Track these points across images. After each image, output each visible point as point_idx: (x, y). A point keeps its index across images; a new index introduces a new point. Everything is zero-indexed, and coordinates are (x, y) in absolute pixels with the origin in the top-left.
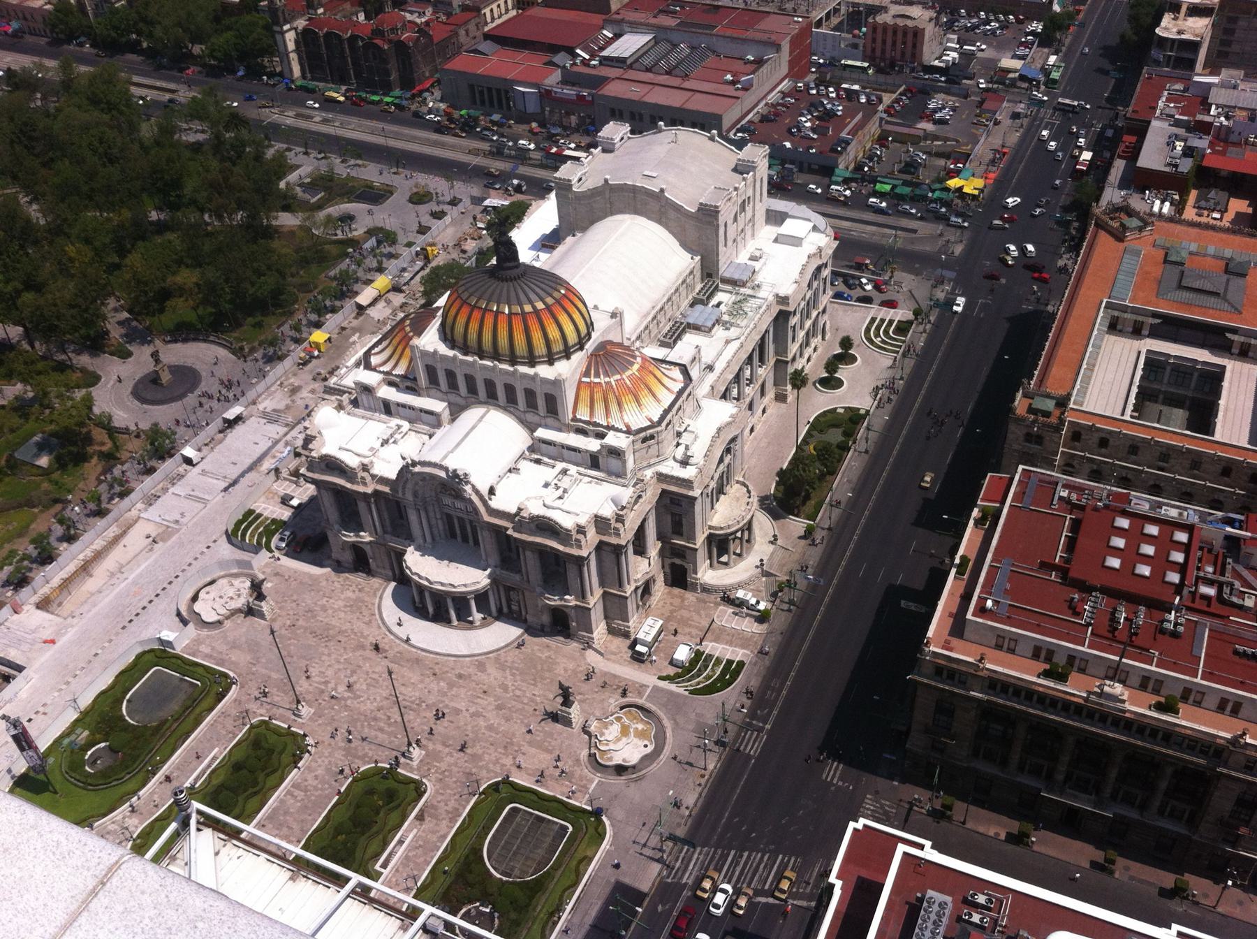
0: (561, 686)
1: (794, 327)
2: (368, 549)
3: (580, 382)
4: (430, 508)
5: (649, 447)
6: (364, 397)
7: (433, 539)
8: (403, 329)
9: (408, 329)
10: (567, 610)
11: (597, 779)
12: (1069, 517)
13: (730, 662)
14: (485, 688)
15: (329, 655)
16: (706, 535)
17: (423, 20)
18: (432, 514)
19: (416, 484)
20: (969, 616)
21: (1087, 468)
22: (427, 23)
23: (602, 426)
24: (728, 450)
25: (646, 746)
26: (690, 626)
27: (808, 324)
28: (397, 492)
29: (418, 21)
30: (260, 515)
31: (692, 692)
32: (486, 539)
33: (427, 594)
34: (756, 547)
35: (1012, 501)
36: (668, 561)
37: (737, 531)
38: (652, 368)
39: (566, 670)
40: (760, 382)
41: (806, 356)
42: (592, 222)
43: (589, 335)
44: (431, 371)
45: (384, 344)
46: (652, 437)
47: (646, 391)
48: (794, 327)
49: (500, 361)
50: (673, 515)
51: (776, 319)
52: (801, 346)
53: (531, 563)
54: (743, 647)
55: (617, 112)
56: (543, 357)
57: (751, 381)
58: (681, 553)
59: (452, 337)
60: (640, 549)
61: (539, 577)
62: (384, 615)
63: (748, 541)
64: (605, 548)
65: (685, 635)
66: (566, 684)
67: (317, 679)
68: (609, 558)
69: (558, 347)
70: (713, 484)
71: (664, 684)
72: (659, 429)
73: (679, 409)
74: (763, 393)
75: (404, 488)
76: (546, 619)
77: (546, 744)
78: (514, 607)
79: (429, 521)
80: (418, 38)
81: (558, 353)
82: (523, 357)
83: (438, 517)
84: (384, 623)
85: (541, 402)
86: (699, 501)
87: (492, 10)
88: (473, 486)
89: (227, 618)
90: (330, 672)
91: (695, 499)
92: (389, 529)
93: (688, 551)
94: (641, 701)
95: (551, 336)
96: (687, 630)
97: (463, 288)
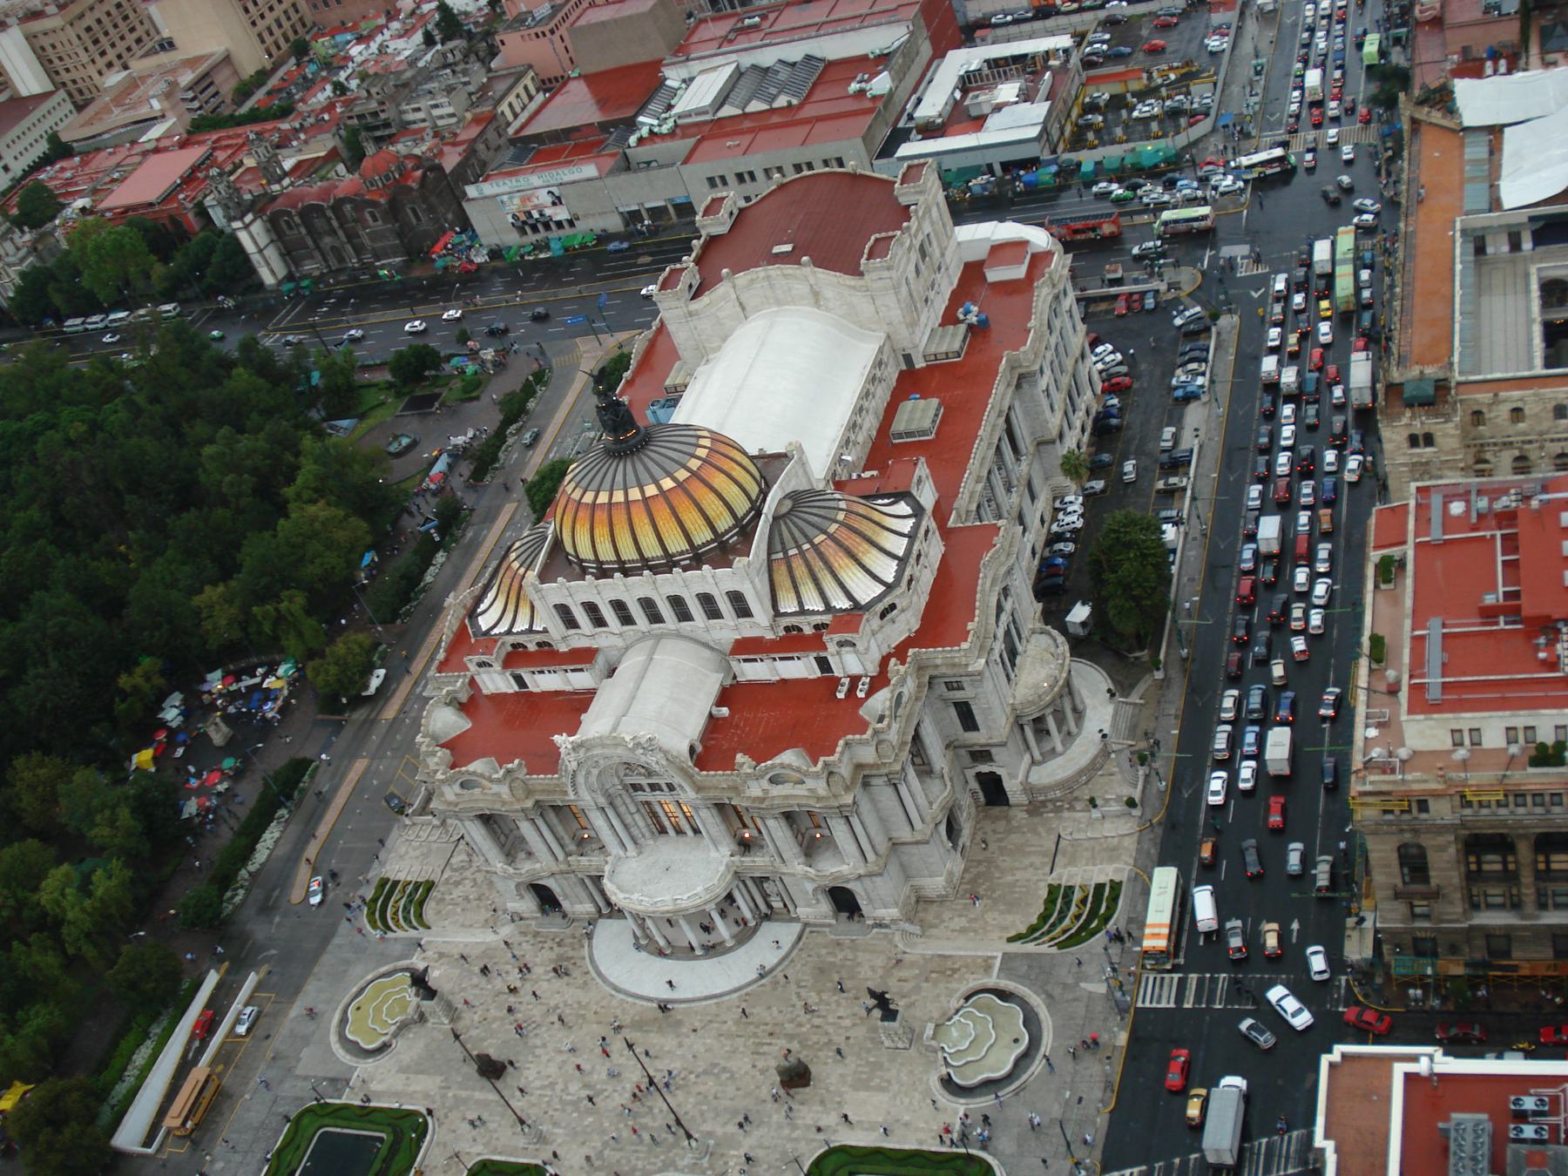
0: (872, 994)
1: (1047, 391)
2: (550, 883)
3: (770, 562)
4: (618, 802)
5: (894, 622)
6: (484, 676)
7: (636, 843)
8: (509, 567)
9: (516, 565)
10: (849, 886)
11: (960, 1106)
12: (1498, 533)
13: (1099, 888)
14: (769, 1028)
15: (544, 1045)
16: (1011, 719)
17: (424, 148)
18: (622, 809)
19: (588, 773)
20: (1404, 717)
21: (1507, 457)
22: (430, 149)
23: (818, 613)
24: (1005, 592)
25: (1016, 1041)
26: (1029, 853)
27: (1065, 380)
28: (566, 793)
29: (417, 151)
30: (396, 883)
31: (1061, 946)
32: (708, 820)
33: (649, 923)
34: (1089, 713)
35: (1416, 536)
36: (970, 773)
37: (1053, 701)
38: (862, 510)
39: (873, 969)
40: (1024, 482)
41: (1078, 424)
42: (724, 339)
43: (764, 494)
44: (564, 612)
45: (491, 595)
46: (893, 607)
47: (866, 546)
48: (1047, 391)
49: (650, 568)
50: (956, 705)
51: (1018, 386)
52: (1066, 413)
53: (777, 831)
54: (1111, 860)
55: (718, 181)
56: (708, 543)
57: (1009, 489)
58: (982, 755)
59: (577, 556)
60: (925, 769)
61: (796, 849)
62: (602, 969)
63: (1075, 710)
64: (874, 781)
65: (1025, 869)
66: (878, 990)
67: (538, 1083)
68: (885, 795)
69: (724, 522)
70: (999, 646)
71: (1016, 947)
72: (898, 591)
73: (919, 556)
74: (1033, 498)
75: (574, 785)
76: (825, 907)
77: (877, 1080)
78: (775, 905)
79: (622, 822)
80: (424, 175)
81: (727, 532)
82: (682, 553)
83: (633, 809)
84: (605, 980)
85: (724, 606)
86: (987, 674)
87: (510, 105)
88: (665, 753)
89: (395, 1035)
90: (552, 1069)
91: (980, 673)
92: (572, 847)
93: (994, 751)
94: (992, 981)
95: (711, 513)
96: (1027, 862)
97: (573, 485)
